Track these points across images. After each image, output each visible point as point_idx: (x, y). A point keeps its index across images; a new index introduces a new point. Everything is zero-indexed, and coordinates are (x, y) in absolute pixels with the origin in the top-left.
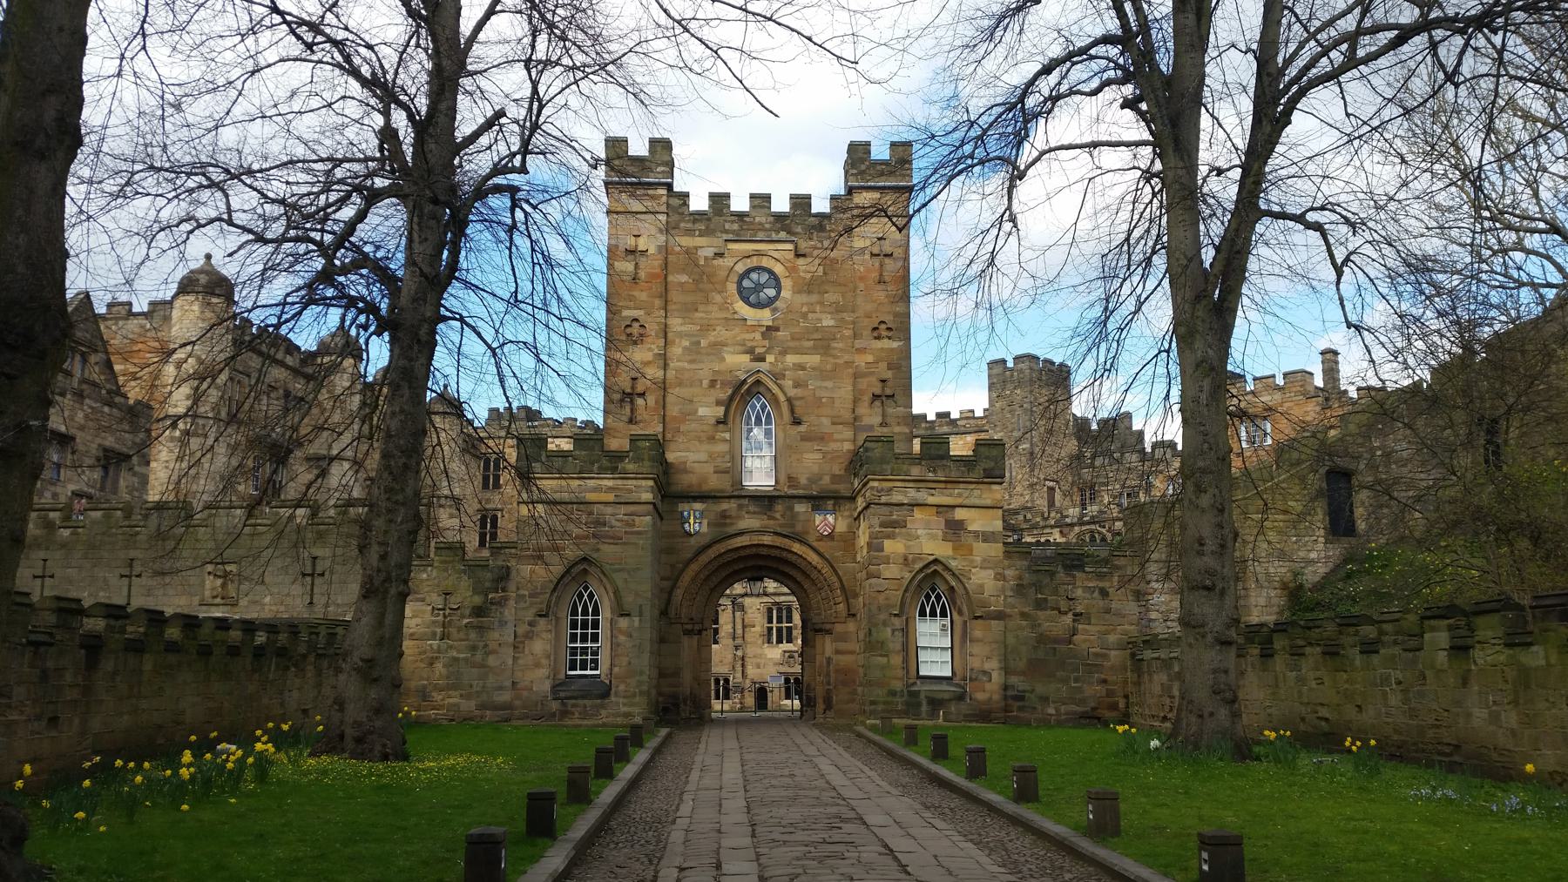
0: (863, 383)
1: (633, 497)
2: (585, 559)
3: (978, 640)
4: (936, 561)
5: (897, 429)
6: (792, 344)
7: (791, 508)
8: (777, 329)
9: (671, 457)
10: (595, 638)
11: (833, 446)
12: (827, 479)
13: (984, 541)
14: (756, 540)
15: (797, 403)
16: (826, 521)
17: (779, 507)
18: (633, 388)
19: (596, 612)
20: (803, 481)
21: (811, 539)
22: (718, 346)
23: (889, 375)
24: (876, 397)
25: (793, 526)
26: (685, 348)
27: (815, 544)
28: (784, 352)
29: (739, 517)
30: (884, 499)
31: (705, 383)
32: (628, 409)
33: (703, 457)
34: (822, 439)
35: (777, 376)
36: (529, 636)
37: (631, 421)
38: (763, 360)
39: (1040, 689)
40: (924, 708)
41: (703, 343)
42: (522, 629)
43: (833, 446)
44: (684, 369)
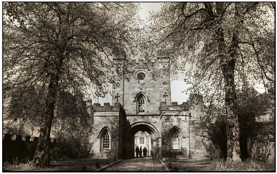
0: (161, 93)
1: (116, 115)
2: (106, 127)
3: (185, 142)
4: (175, 126)
5: (168, 102)
6: (148, 86)
7: (148, 117)
8: (145, 84)
9: (124, 108)
10: (108, 142)
11: (156, 105)
12: (155, 112)
13: (185, 122)
14: (141, 123)
15: (148, 97)
16: (154, 119)
17: (146, 117)
18: (118, 95)
19: (108, 137)
20: (150, 112)
21: (152, 123)
22: (133, 87)
23: (166, 92)
24: (164, 96)
25: (148, 121)
26: (127, 88)
27: (153, 124)
28: (146, 88)
29: (138, 119)
30: (165, 114)
31: (131, 94)
32: (117, 99)
33: (131, 108)
34: (154, 104)
35: (145, 93)
36: (95, 141)
37: (117, 101)
38: (142, 89)
39: (197, 151)
40: (174, 155)
41: (131, 87)
42: (94, 140)
43: (156, 105)
44: (127, 92)
